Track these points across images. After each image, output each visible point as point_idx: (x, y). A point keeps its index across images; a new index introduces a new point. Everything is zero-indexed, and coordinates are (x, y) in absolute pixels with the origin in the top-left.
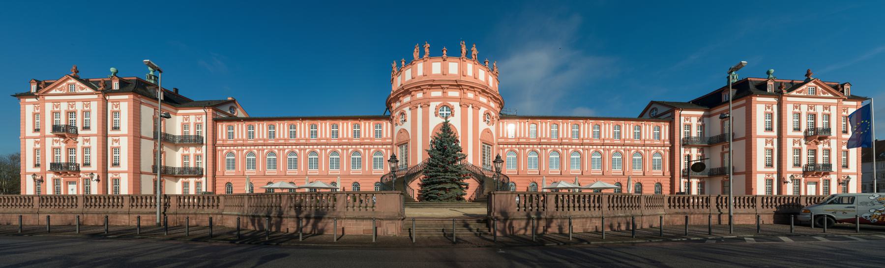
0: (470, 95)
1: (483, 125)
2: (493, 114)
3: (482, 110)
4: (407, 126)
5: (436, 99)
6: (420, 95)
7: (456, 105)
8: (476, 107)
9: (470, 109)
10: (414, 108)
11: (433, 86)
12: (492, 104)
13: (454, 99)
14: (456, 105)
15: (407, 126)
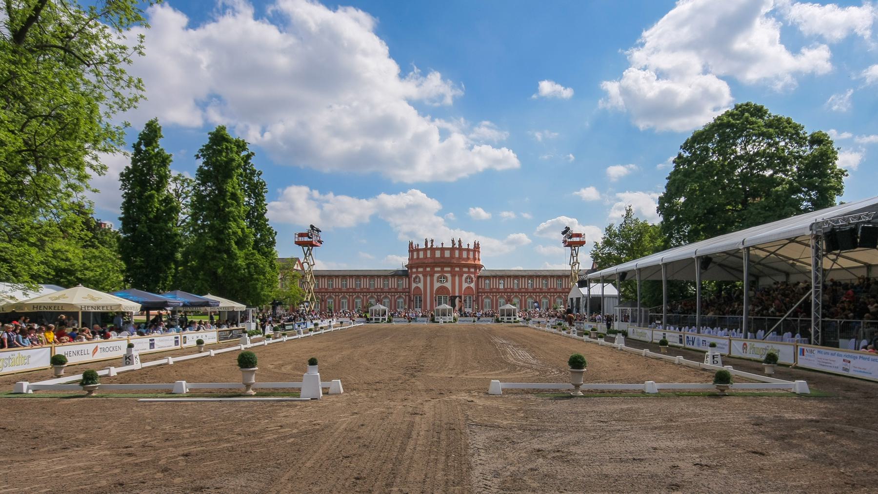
0: (457, 269)
1: (465, 285)
2: (473, 276)
3: (465, 275)
4: (421, 285)
5: (438, 272)
6: (428, 269)
7: (448, 275)
8: (461, 276)
9: (457, 278)
10: (425, 276)
11: (436, 264)
12: (472, 270)
13: (447, 272)
14: (448, 275)
15: (421, 285)
